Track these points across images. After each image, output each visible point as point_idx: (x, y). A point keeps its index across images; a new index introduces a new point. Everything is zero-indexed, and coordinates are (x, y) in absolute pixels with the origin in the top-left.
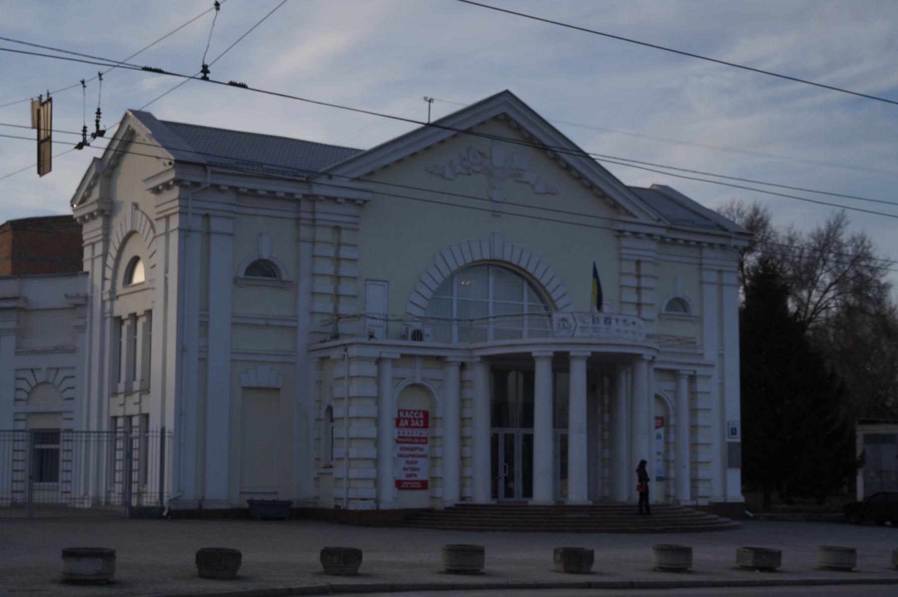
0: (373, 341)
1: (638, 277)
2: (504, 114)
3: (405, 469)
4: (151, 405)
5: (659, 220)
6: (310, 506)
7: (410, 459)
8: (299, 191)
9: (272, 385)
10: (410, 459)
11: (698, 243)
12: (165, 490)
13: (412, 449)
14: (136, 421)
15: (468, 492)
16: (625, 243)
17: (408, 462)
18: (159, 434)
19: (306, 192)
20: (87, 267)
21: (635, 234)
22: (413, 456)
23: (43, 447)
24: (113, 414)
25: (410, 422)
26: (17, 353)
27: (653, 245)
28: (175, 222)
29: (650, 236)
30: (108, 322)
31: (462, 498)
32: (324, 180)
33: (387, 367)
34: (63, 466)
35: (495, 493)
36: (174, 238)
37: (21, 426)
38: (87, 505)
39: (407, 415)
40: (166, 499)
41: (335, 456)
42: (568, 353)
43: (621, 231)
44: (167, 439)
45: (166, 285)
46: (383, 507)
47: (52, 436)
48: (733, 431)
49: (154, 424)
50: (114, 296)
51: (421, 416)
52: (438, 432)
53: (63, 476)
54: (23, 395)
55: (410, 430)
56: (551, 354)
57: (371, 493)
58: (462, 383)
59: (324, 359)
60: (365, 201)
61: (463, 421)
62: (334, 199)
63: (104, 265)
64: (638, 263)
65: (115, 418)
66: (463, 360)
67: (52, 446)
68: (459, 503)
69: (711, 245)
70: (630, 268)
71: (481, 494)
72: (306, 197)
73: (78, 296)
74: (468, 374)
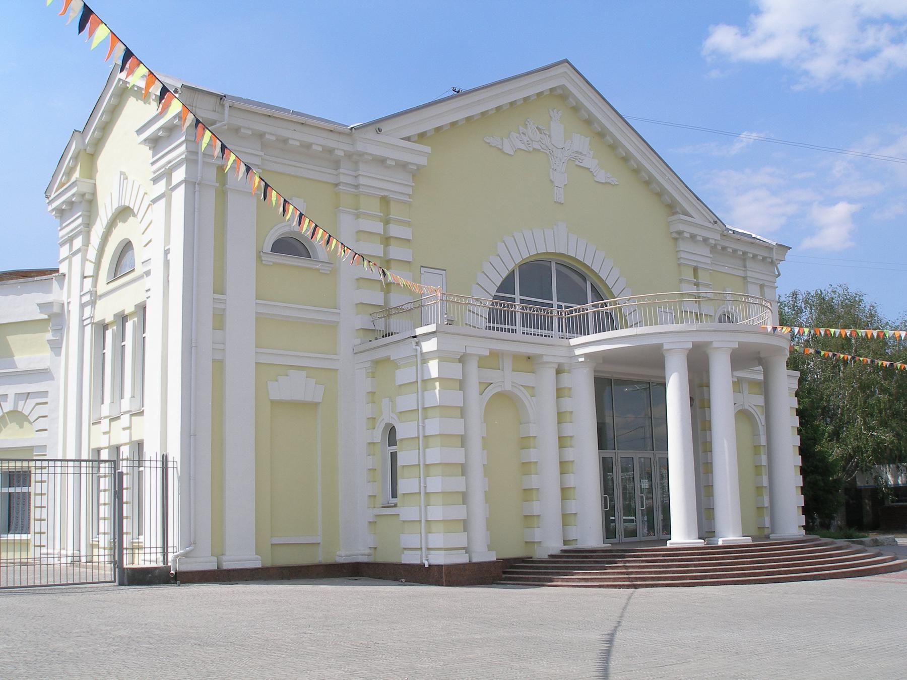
2: (563, 87)
4: (147, 429)
5: (716, 222)
8: (341, 147)
9: (309, 398)
11: (745, 253)
12: (170, 544)
14: (125, 452)
15: (573, 534)
16: (683, 246)
18: (159, 464)
19: (347, 148)
21: (693, 237)
23: (12, 490)
24: (94, 445)
27: (706, 251)
28: (180, 175)
29: (705, 240)
30: (88, 330)
31: (566, 542)
32: (371, 134)
33: (473, 366)
34: (35, 514)
35: (609, 532)
36: (179, 196)
40: (171, 557)
41: (401, 490)
42: (708, 344)
43: (680, 233)
44: (170, 471)
45: (167, 263)
46: (475, 560)
49: (152, 451)
50: (95, 298)
53: (35, 526)
57: (460, 539)
58: (560, 393)
59: (376, 363)
60: (419, 167)
61: (563, 442)
62: (381, 161)
63: (84, 260)
64: (695, 270)
66: (562, 360)
67: (25, 490)
69: (755, 256)
70: (689, 275)
71: (591, 535)
72: (349, 156)
74: (566, 380)
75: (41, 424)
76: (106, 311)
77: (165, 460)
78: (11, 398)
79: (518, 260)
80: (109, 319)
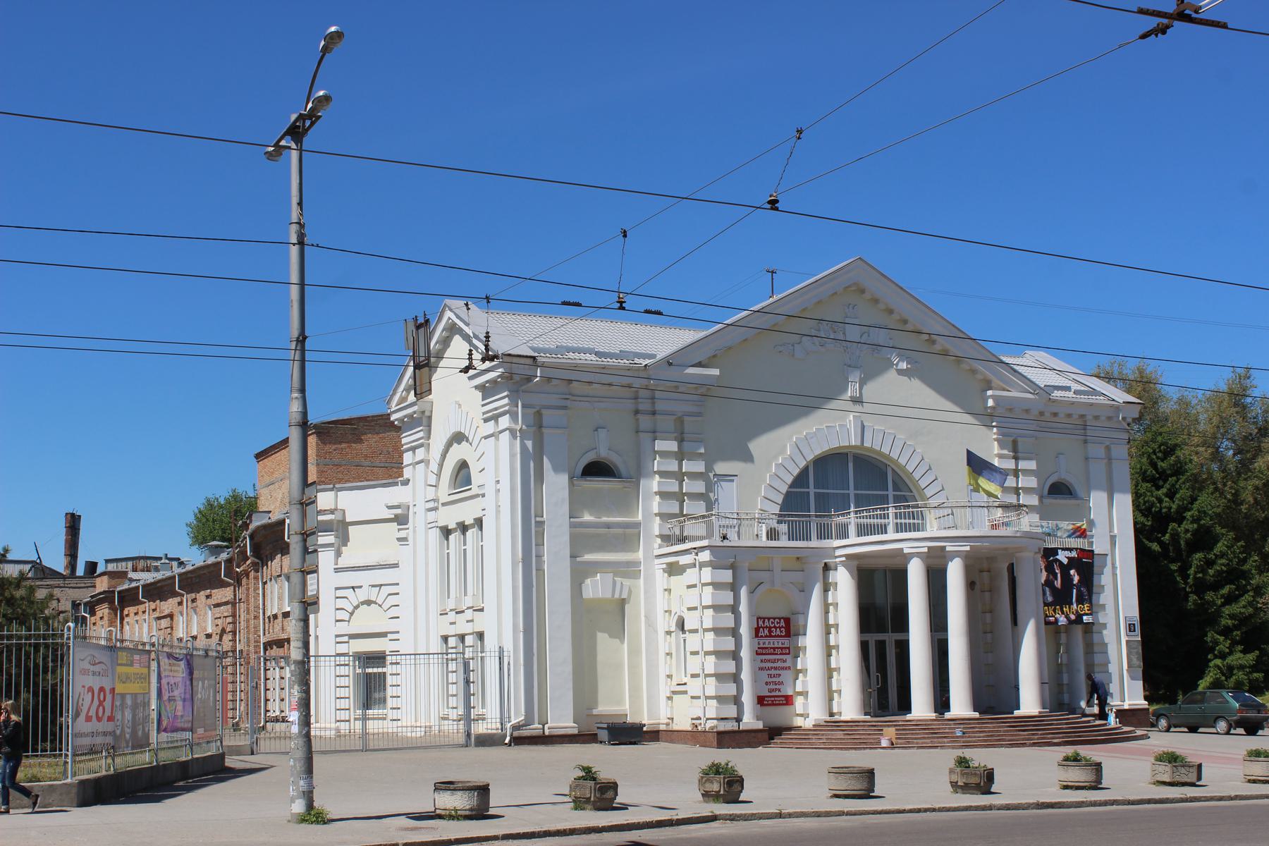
0: (726, 543)
1: (1016, 458)
3: (767, 683)
6: (663, 727)
7: (773, 672)
10: (773, 672)
13: (774, 661)
17: (770, 676)
20: (407, 473)
22: (775, 668)
25: (770, 631)
26: (337, 570)
34: (390, 691)
37: (342, 649)
38: (419, 733)
39: (767, 624)
47: (378, 658)
48: (1131, 628)
49: (491, 643)
51: (783, 623)
52: (801, 641)
53: (391, 702)
54: (345, 616)
55: (771, 640)
56: (925, 550)
57: (732, 711)
65: (445, 639)
67: (380, 670)
68: (828, 719)
71: (849, 706)
73: (398, 507)
74: (833, 577)
75: (394, 612)
76: (449, 517)
77: (501, 650)
78: (365, 587)
79: (810, 457)
80: (452, 526)
